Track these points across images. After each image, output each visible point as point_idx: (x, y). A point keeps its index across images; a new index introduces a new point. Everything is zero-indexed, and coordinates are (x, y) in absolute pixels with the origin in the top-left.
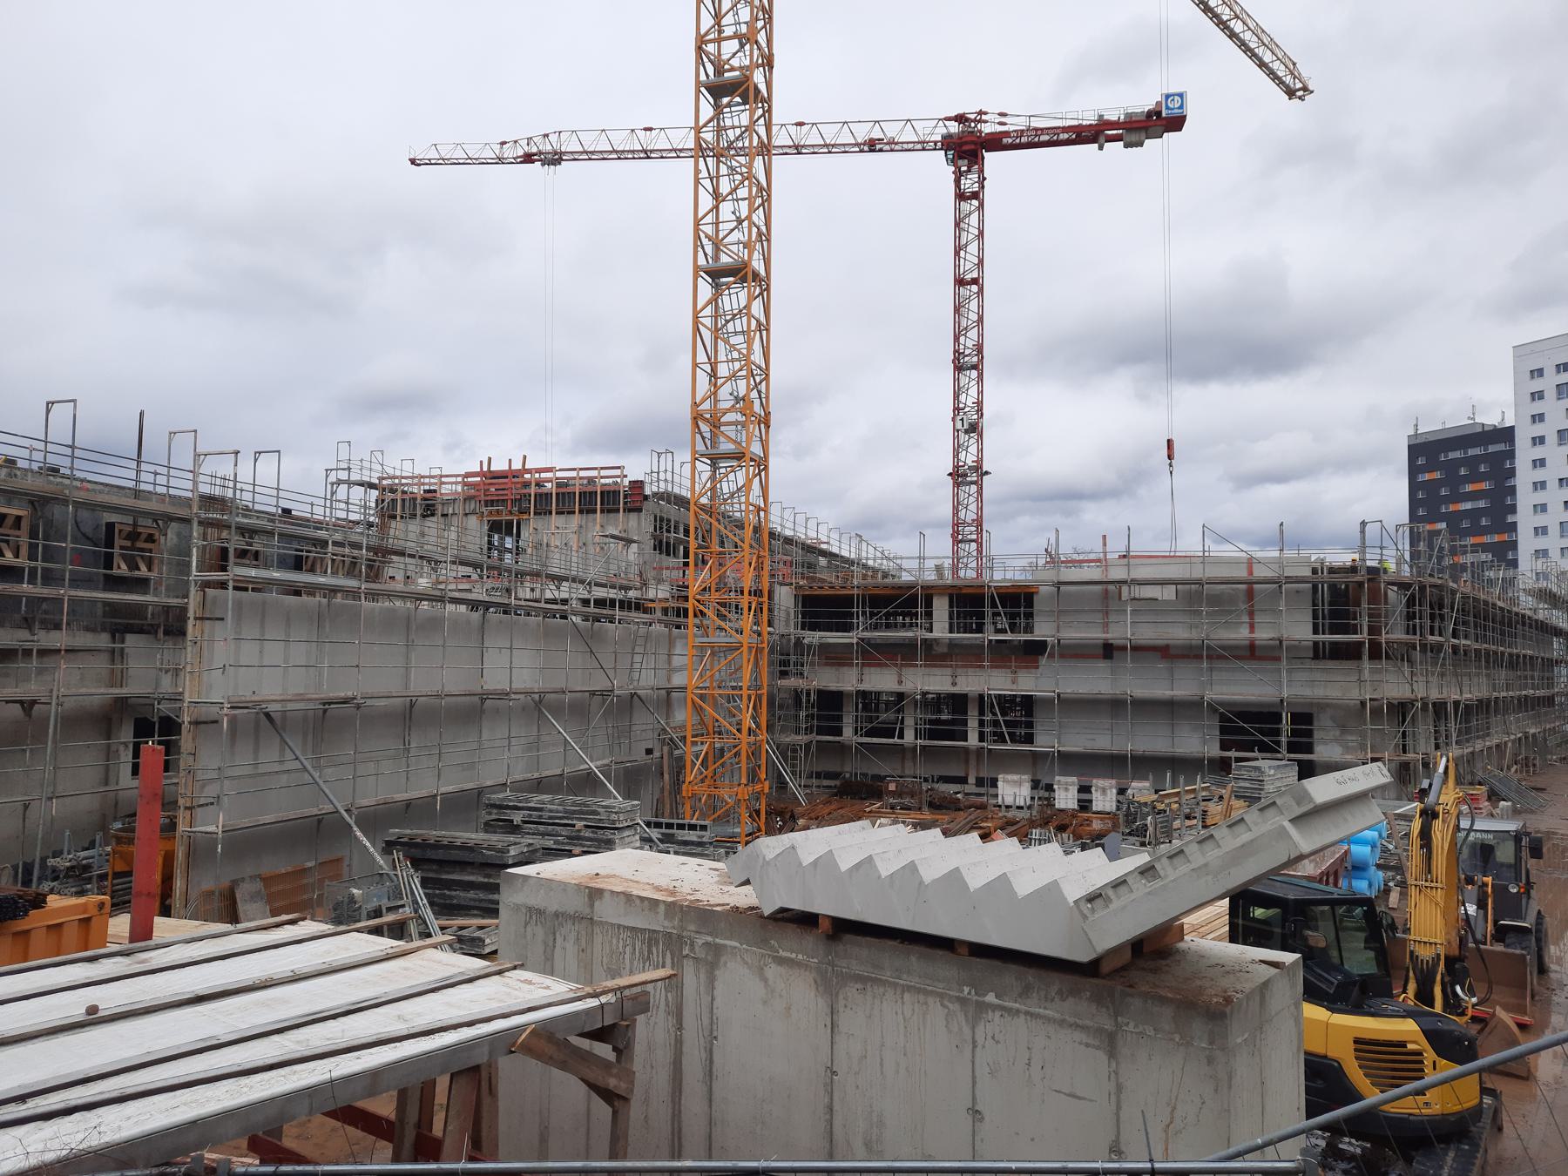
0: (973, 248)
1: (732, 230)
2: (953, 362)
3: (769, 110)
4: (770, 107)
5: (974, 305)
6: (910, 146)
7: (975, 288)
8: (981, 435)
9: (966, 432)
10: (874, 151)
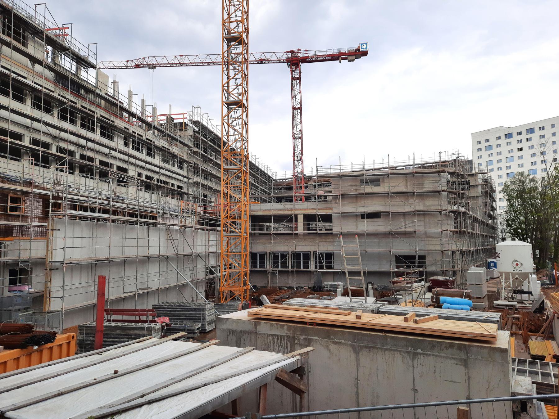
1: (234, 89)
2: (293, 136)
3: (248, 48)
4: (248, 46)
6: (275, 61)
7: (299, 111)
8: (303, 162)
9: (298, 161)
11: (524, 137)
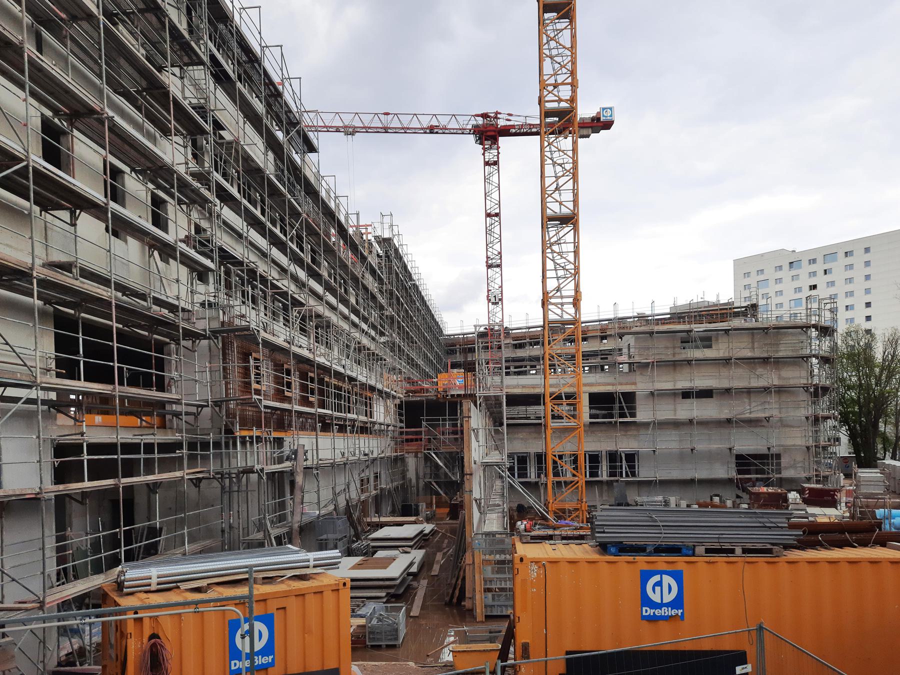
6: (455, 131)
10: (432, 133)
11: (819, 267)
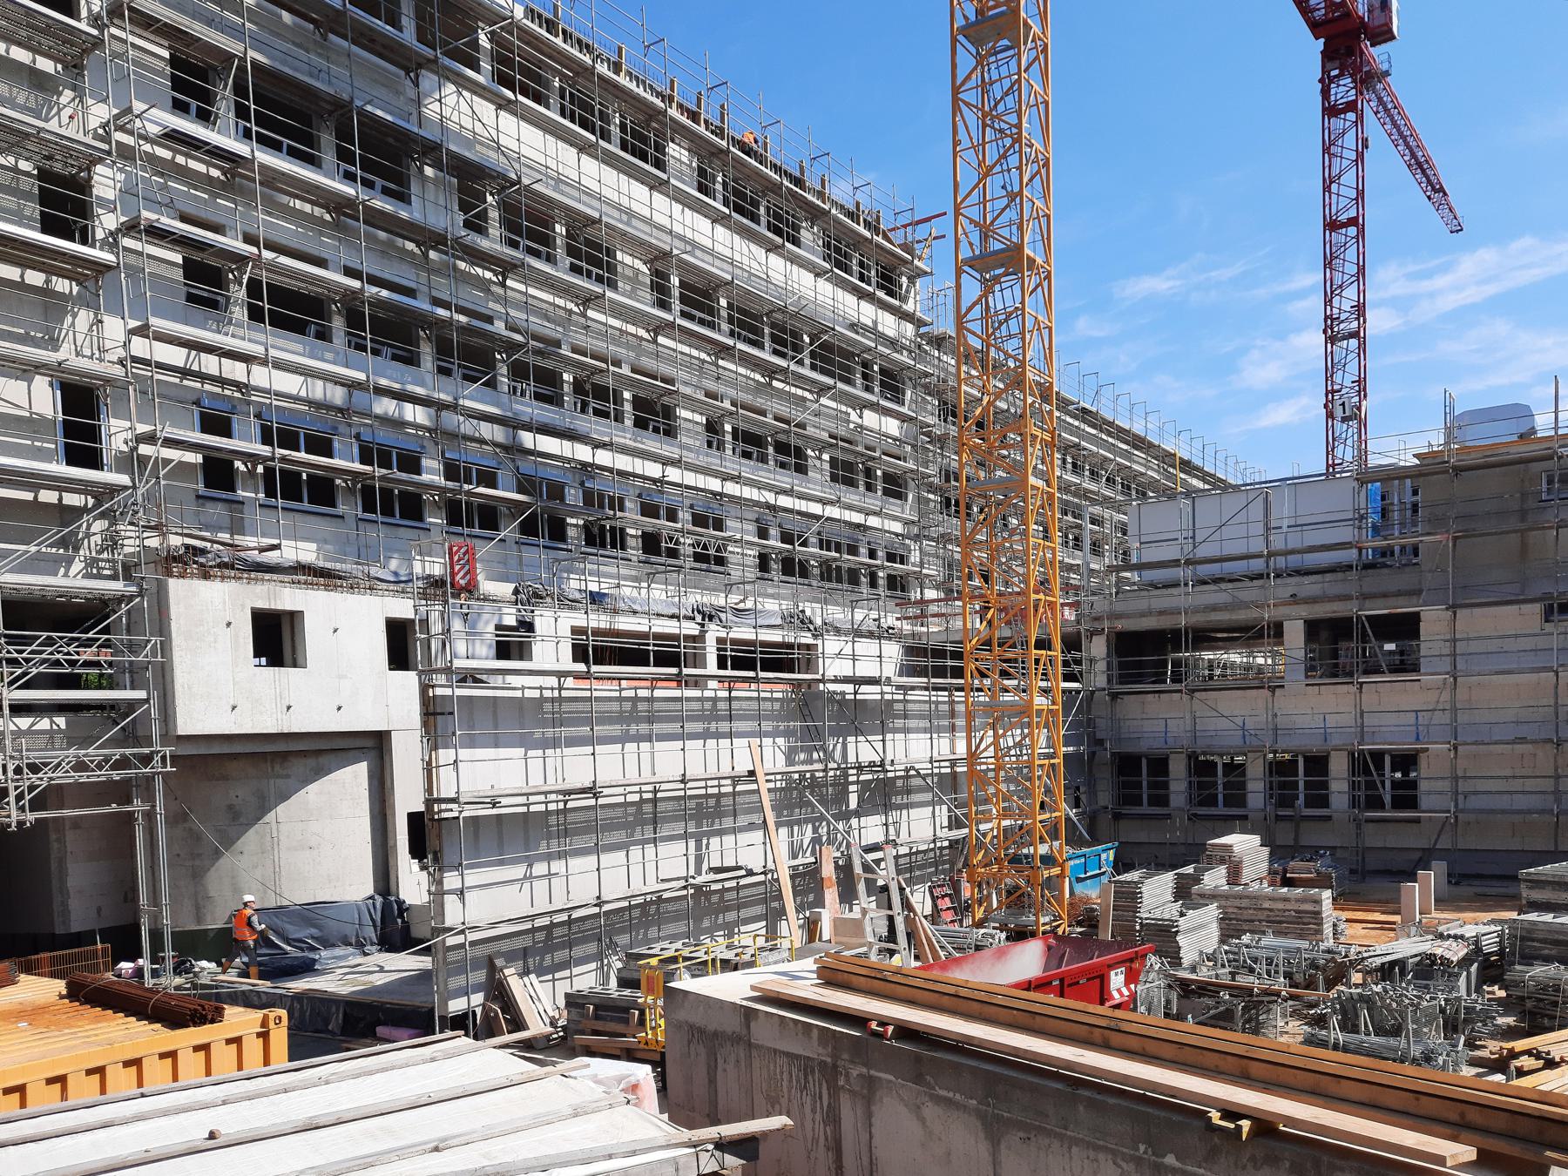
0: (1349, 178)
2: (1325, 332)
5: (1351, 254)
7: (1352, 231)
8: (1362, 424)
9: (1344, 420)
